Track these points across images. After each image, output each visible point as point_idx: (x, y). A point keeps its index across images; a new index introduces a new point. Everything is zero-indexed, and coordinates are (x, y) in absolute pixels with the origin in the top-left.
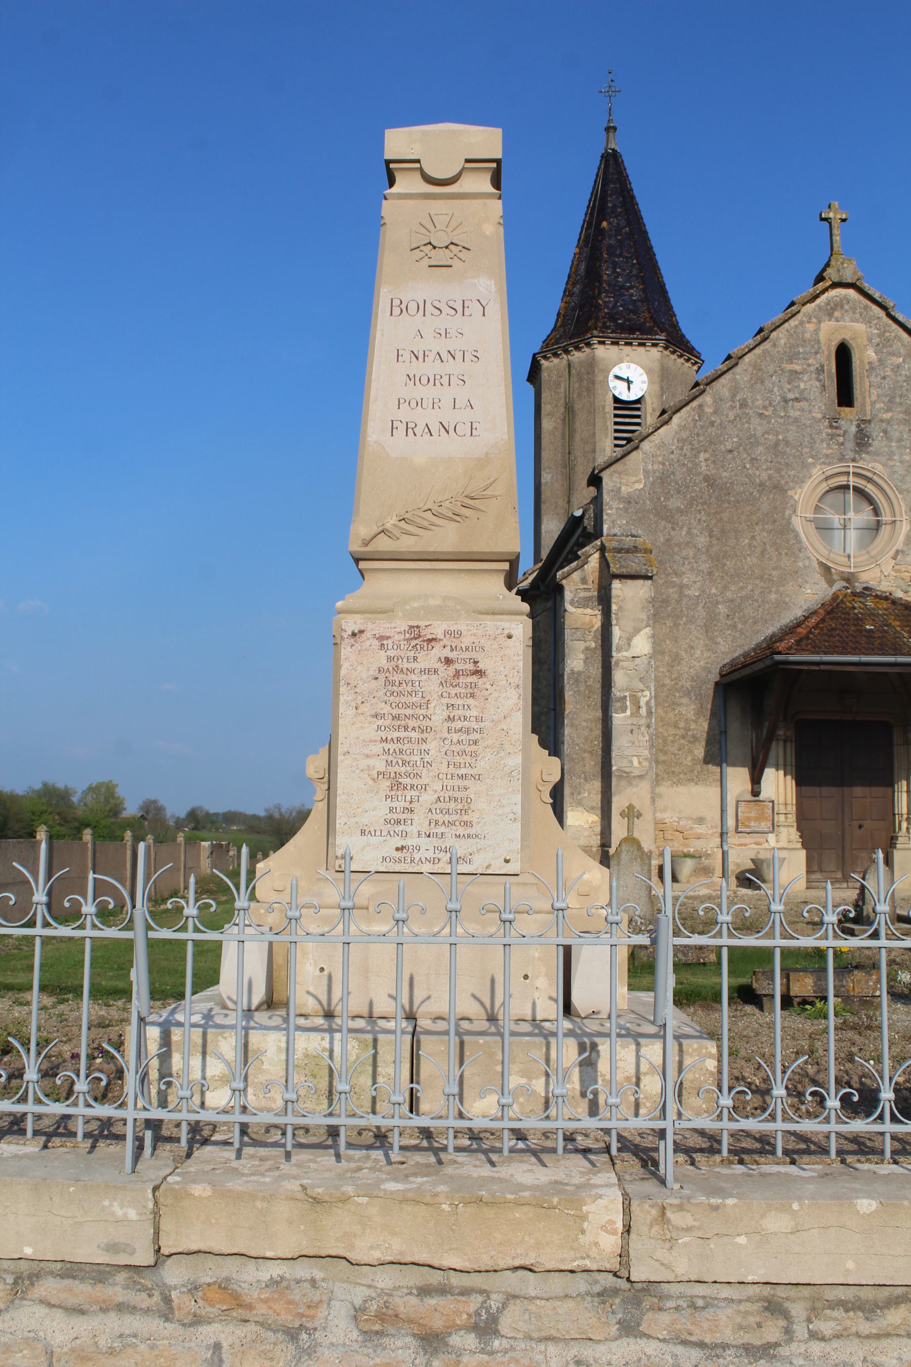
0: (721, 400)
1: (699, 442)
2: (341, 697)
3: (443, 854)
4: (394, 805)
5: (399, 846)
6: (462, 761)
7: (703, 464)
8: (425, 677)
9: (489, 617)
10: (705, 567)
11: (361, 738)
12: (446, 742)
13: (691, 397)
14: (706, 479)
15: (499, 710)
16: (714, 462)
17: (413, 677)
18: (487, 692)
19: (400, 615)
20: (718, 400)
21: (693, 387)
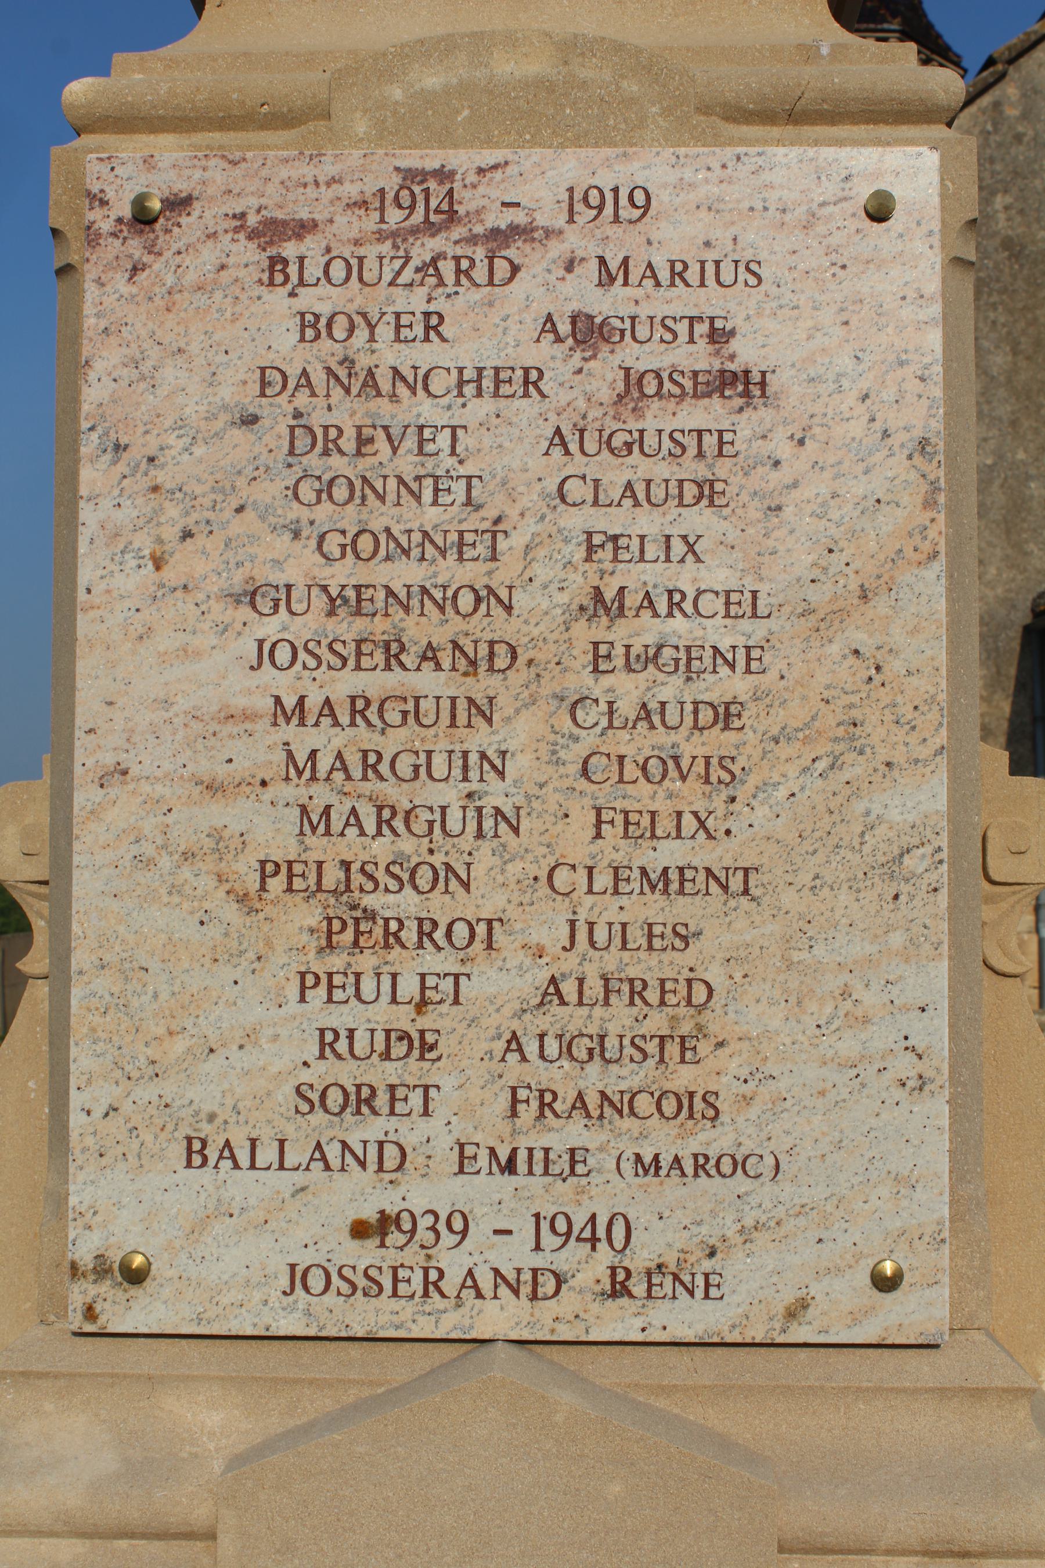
0: (1036, 92)
1: (993, 174)
2: (87, 513)
3: (577, 1251)
4: (340, 1018)
5: (369, 1213)
6: (664, 806)
7: (1002, 216)
8: (481, 408)
9: (775, 131)
10: (1004, 411)
11: (182, 704)
12: (588, 715)
13: (980, 86)
14: (1007, 244)
15: (837, 560)
16: (1021, 212)
17: (427, 410)
18: (776, 477)
19: (361, 128)
20: (1030, 93)
21: (985, 67)
